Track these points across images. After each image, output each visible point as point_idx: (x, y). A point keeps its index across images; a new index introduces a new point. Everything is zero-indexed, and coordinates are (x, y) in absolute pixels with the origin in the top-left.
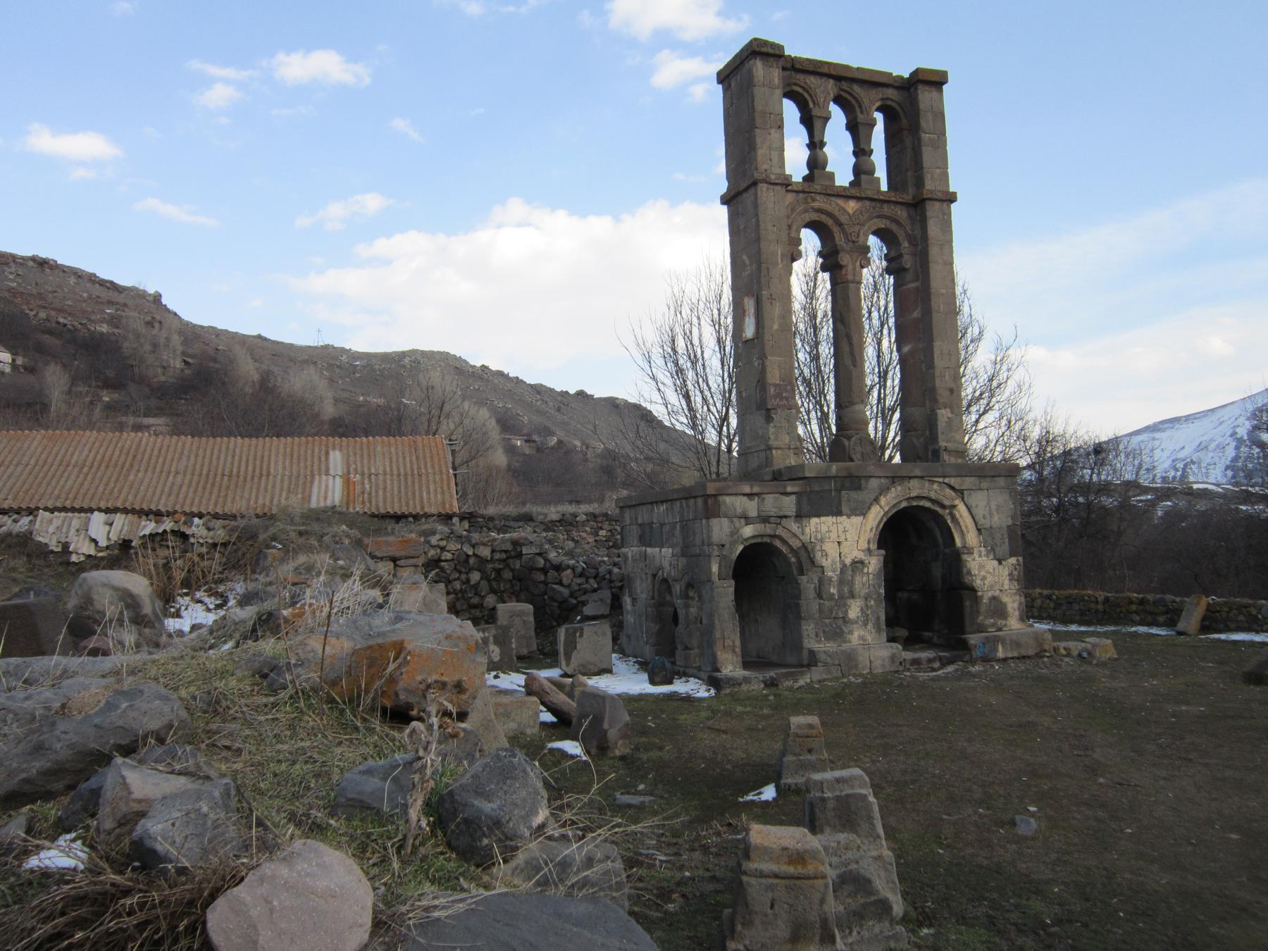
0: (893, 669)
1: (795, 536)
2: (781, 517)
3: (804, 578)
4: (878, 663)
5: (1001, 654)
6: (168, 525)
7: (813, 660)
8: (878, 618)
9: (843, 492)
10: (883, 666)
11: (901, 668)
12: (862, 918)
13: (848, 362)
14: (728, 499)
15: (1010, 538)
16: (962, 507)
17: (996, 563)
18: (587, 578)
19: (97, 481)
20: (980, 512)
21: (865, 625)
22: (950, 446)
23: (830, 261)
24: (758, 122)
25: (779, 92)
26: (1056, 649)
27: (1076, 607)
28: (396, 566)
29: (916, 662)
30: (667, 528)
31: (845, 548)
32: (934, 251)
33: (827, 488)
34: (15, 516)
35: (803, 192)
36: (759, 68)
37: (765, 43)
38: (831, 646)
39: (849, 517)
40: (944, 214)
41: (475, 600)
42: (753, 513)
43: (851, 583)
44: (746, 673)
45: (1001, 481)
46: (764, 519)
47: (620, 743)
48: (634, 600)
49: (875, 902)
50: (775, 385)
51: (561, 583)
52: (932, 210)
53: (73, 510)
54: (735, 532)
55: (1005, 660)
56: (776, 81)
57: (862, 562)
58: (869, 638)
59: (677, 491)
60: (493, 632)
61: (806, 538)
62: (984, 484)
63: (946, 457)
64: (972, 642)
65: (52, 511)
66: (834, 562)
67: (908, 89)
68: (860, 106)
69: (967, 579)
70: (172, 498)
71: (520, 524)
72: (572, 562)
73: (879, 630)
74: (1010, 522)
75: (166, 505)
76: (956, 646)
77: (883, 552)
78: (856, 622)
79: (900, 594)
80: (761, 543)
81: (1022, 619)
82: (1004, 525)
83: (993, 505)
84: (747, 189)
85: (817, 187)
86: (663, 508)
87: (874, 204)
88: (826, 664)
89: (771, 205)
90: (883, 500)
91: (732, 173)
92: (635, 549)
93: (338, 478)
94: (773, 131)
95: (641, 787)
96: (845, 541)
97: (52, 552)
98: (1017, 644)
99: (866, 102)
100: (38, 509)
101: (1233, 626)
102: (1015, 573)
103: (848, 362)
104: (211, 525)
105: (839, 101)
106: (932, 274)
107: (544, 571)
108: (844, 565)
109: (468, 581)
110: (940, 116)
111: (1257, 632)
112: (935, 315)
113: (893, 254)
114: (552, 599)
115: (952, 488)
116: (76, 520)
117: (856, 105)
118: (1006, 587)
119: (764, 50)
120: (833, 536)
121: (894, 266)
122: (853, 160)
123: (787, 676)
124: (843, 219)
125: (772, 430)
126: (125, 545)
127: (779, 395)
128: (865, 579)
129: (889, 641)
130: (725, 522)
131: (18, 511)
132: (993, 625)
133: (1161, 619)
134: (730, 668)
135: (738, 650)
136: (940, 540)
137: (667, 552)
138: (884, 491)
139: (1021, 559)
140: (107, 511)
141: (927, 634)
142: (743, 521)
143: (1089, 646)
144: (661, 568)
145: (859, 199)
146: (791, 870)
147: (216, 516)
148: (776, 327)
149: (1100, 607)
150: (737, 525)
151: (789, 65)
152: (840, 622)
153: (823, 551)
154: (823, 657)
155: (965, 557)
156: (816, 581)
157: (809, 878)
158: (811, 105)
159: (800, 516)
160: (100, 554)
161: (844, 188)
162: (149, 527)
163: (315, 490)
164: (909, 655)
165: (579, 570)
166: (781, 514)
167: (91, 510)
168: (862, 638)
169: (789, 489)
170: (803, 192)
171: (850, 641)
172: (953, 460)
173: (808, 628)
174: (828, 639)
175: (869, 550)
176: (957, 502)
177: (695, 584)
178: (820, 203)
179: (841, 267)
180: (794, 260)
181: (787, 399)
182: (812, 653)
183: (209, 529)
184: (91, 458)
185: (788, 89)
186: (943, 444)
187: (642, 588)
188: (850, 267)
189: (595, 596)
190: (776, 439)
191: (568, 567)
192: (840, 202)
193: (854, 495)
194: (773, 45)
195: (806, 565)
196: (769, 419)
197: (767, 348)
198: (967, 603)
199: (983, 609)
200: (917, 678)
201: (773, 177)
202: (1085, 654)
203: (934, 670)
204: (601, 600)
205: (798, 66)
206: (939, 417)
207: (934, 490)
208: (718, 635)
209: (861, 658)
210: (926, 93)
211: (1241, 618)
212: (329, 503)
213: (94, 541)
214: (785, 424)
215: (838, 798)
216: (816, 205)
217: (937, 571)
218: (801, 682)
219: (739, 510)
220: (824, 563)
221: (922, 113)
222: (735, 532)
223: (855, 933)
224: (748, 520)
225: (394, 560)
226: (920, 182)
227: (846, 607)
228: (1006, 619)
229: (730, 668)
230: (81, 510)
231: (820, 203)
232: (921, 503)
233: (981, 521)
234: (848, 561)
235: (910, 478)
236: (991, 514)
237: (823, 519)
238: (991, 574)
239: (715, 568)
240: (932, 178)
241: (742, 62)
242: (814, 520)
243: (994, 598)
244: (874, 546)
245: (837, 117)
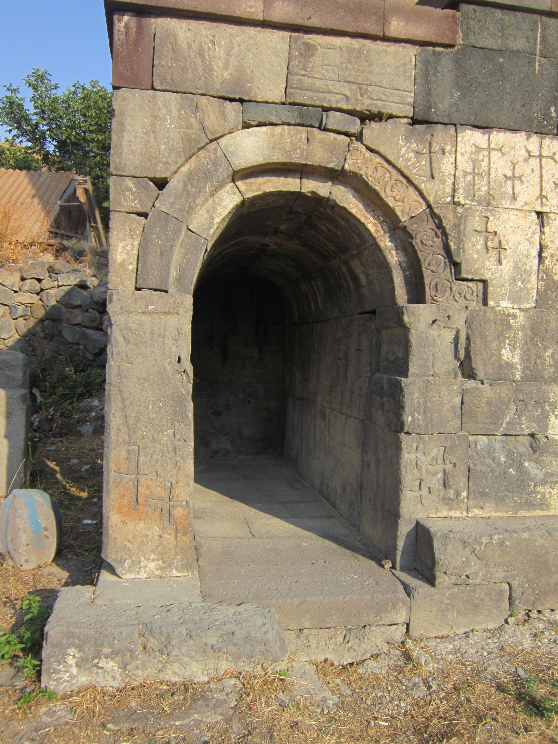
2: (366, 117)
33: (519, 44)
42: (270, 89)
66: (519, 271)
80: (299, 195)
120: (527, 193)
134: (152, 566)
153: (488, 234)
156: (460, 322)
166: (364, 104)
169: (396, 27)
171: (544, 505)
174: (479, 495)
220: (489, 269)
237: (499, 137)
242: (472, 138)
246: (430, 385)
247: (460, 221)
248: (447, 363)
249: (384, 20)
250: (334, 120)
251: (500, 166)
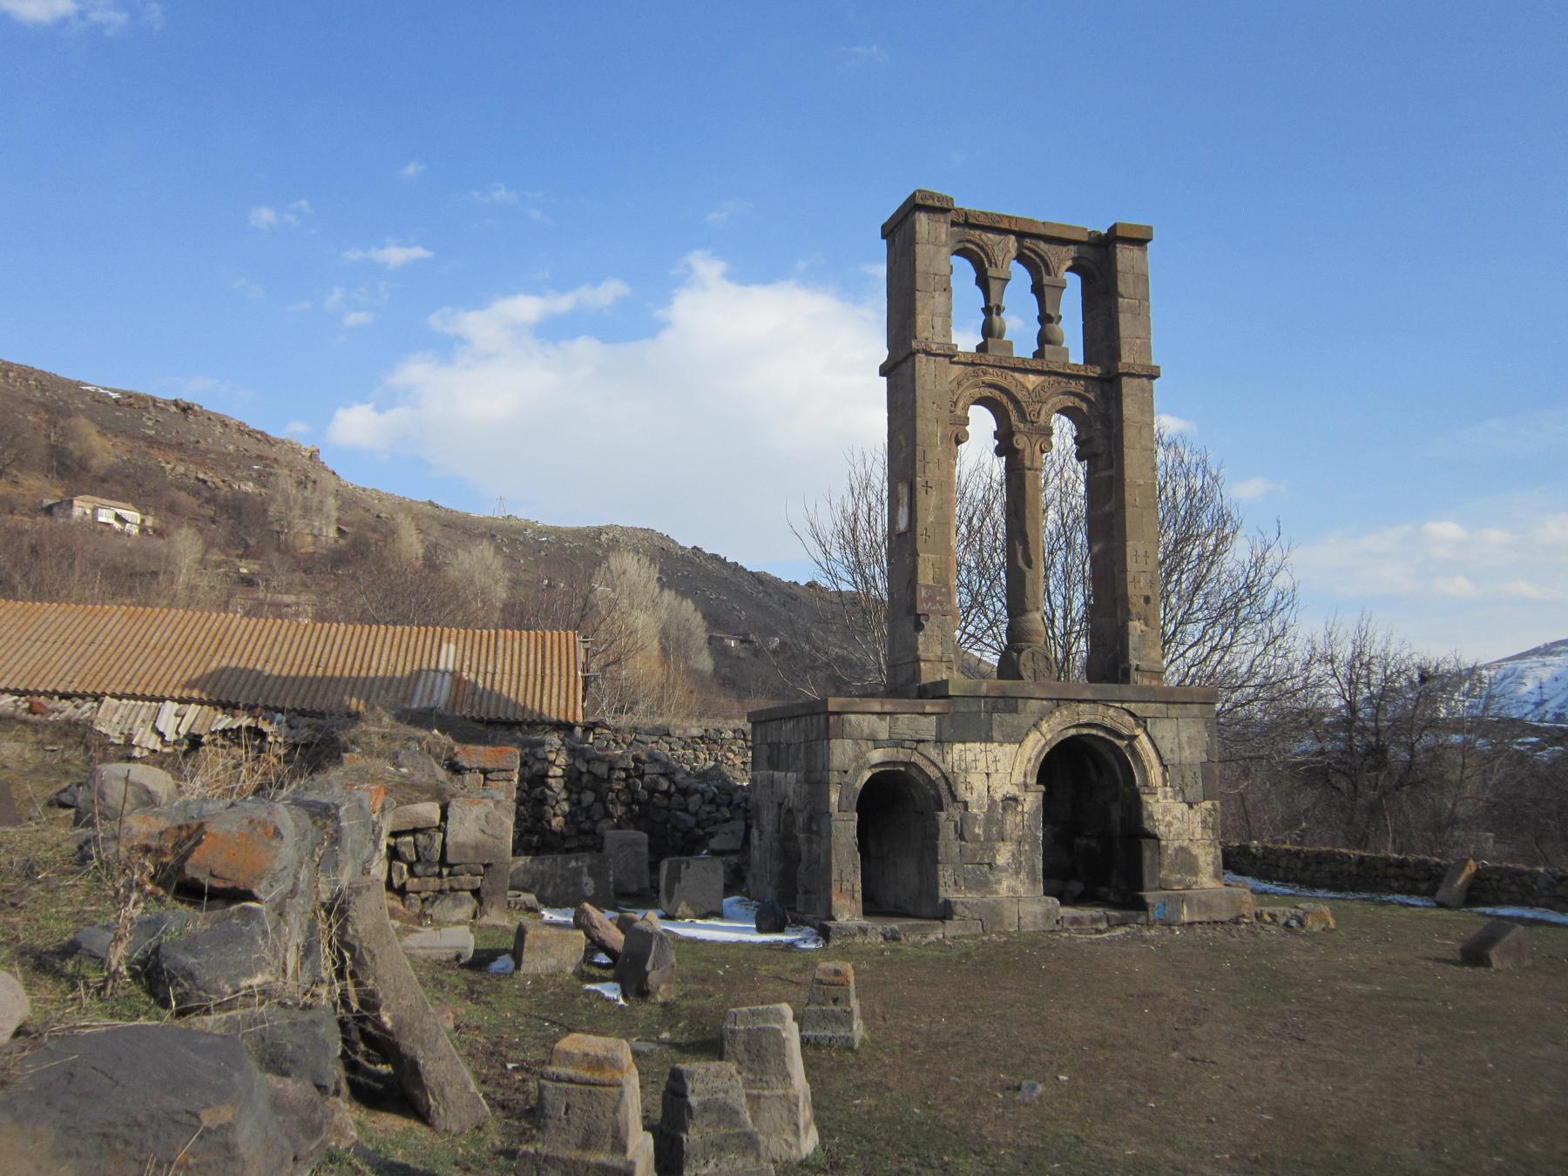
0: (1048, 928)
1: (934, 764)
2: (918, 741)
3: (943, 815)
4: (1027, 920)
5: (1186, 916)
6: (245, 721)
7: (945, 912)
8: (1033, 866)
9: (995, 715)
10: (1035, 924)
11: (1058, 928)
12: (722, 1149)
13: (1021, 563)
14: (852, 717)
15: (1204, 778)
16: (1143, 738)
17: (1185, 806)
18: (719, 806)
19: (175, 666)
20: (1165, 746)
21: (1017, 873)
22: (1143, 665)
23: (1005, 445)
24: (920, 282)
25: (945, 250)
26: (1259, 916)
27: (1326, 868)
28: (486, 779)
29: (1075, 921)
30: (792, 749)
31: (995, 780)
32: (1129, 434)
33: (975, 709)
34: (79, 701)
35: (973, 364)
36: (922, 221)
37: (932, 195)
38: (972, 896)
39: (1001, 744)
40: (1144, 391)
41: (587, 826)
42: (884, 736)
43: (1001, 823)
44: (864, 922)
45: (1195, 709)
46: (898, 743)
47: (662, 988)
48: (761, 833)
49: (738, 1135)
50: (927, 587)
51: (686, 810)
52: (1128, 386)
53: (143, 698)
54: (859, 756)
55: (1191, 924)
56: (943, 237)
57: (1015, 799)
58: (1021, 890)
59: (803, 705)
60: (588, 860)
61: (945, 768)
62: (1174, 711)
63: (1134, 675)
64: (1149, 900)
65: (120, 698)
66: (980, 796)
67: (1107, 247)
68: (1047, 266)
69: (1147, 825)
70: (256, 690)
71: (655, 738)
72: (702, 786)
73: (1034, 881)
74: (1204, 758)
75: (248, 697)
76: (1131, 902)
77: (1042, 787)
78: (1006, 870)
79: (1078, 841)
81: (1216, 876)
82: (1197, 762)
83: (1184, 737)
84: (905, 359)
85: (990, 358)
86: (791, 724)
88: (963, 918)
90: (1044, 726)
91: (891, 345)
92: (764, 772)
93: (447, 677)
95: (665, 1035)
96: (996, 773)
97: (112, 744)
98: (1206, 906)
99: (1053, 261)
100: (104, 694)
101: (1504, 897)
102: (1210, 820)
103: (1021, 563)
104: (294, 722)
105: (1020, 258)
106: (1127, 461)
107: (667, 794)
108: (993, 802)
109: (579, 802)
110: (1143, 278)
111: (1531, 906)
112: (1129, 511)
113: (1084, 437)
114: (674, 828)
115: (1132, 715)
116: (146, 708)
118: (1198, 836)
119: (929, 202)
120: (981, 765)
121: (1085, 450)
122: (1039, 327)
123: (913, 929)
125: (921, 639)
126: (195, 742)
127: (931, 599)
128: (1019, 818)
129: (1046, 893)
130: (849, 742)
131: (83, 696)
132: (1179, 882)
133: (1423, 887)
135: (859, 896)
136: (1120, 776)
137: (792, 776)
138: (1045, 715)
139: (1217, 803)
140: (181, 701)
141: (1104, 890)
142: (870, 744)
143: (1300, 913)
144: (786, 796)
146: (587, 1075)
147: (302, 713)
148: (931, 519)
149: (1354, 870)
150: (864, 748)
151: (961, 220)
152: (986, 868)
154: (959, 909)
155: (1144, 798)
157: (604, 1085)
159: (940, 741)
160: (167, 750)
161: (1024, 360)
162: (223, 721)
163: (420, 687)
164: (1068, 912)
165: (710, 795)
167: (163, 699)
168: (1011, 889)
169: (928, 709)
170: (973, 364)
172: (1146, 682)
173: (945, 875)
174: (969, 888)
175: (1026, 786)
176: (1138, 731)
177: (818, 815)
178: (992, 376)
179: (1017, 451)
180: (958, 442)
181: (941, 603)
182: (947, 903)
183: (291, 727)
184: (172, 641)
185: (960, 246)
186: (1134, 662)
187: (768, 818)
188: (1028, 451)
189: (726, 827)
190: (927, 650)
191: (696, 791)
192: (1018, 376)
193: (1008, 717)
194: (940, 198)
195: (946, 799)
196: (919, 627)
197: (920, 545)
198: (1147, 854)
199: (1166, 861)
200: (1074, 939)
201: (934, 347)
202: (1294, 923)
203: (1099, 931)
204: (733, 833)
205: (972, 220)
206: (1131, 630)
207: (1111, 716)
208: (835, 876)
209: (1007, 913)
211: (1513, 888)
212: (432, 705)
213: (162, 735)
214: (937, 632)
215: (749, 1031)
216: (988, 379)
217: (1116, 813)
218: (932, 938)
219: (866, 731)
220: (968, 797)
221: (1120, 275)
222: (859, 756)
223: (712, 1163)
224: (877, 743)
225: (485, 772)
226: (1115, 355)
227: (993, 851)
228: (1196, 875)
229: (847, 916)
230: (152, 699)
232: (1094, 732)
233: (1167, 756)
234: (998, 797)
235: (1080, 701)
236: (1180, 748)
237: (969, 745)
238: (1178, 820)
239: (834, 798)
241: (906, 216)
242: (958, 747)
243: (1181, 849)
244: (1032, 780)
245: (1020, 277)
246: (948, 843)
247: (955, 779)
248: (952, 835)
249: (923, 706)
250: (907, 744)
251: (970, 756)
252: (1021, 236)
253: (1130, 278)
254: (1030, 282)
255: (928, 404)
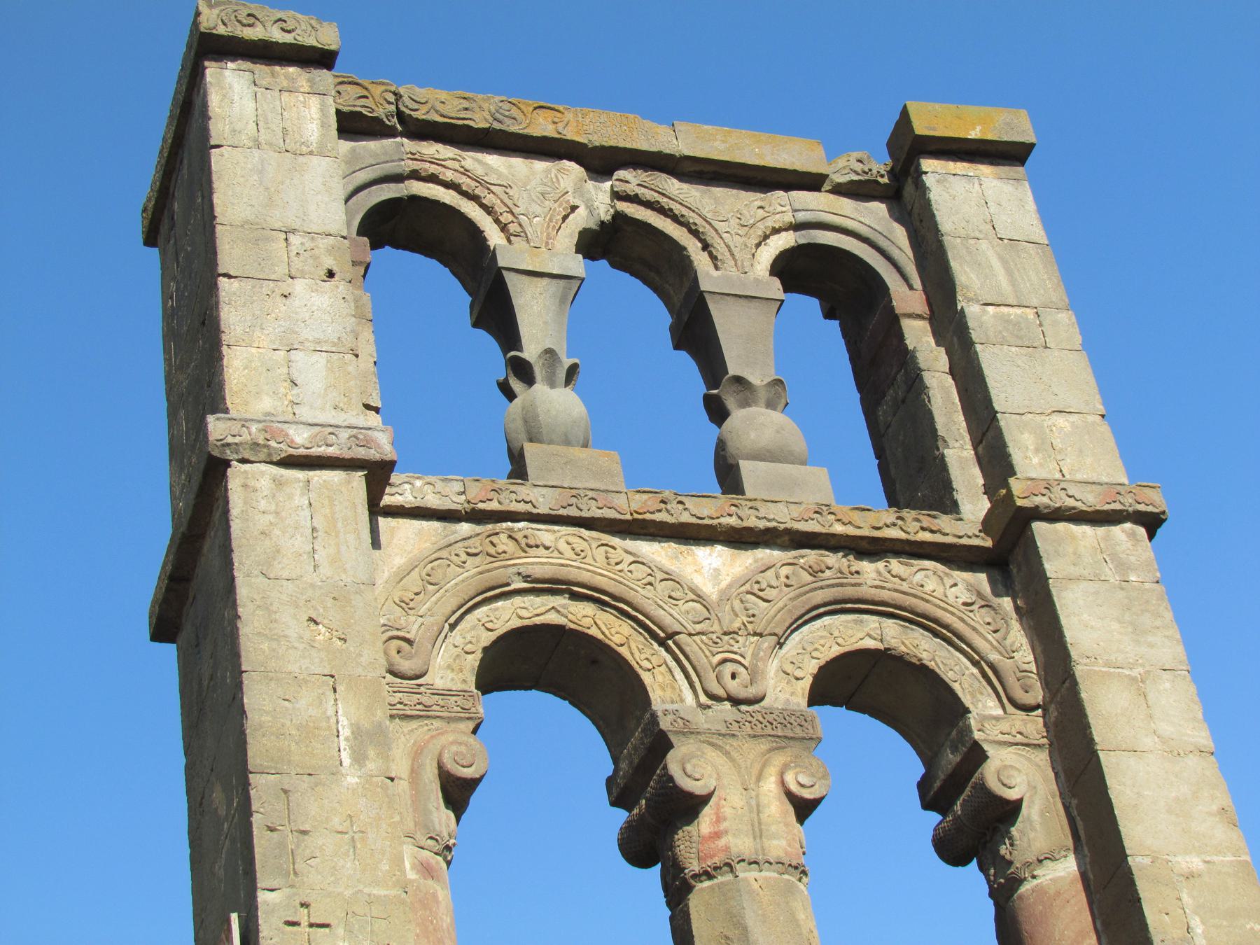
24: (230, 254)
36: (231, 90)
40: (1122, 567)
87: (810, 556)
89: (300, 543)
94: (299, 286)
117: (692, 246)
124: (674, 616)
145: (740, 539)
158: (495, 238)
170: (477, 516)
178: (561, 550)
210: (959, 186)
216: (539, 564)
231: (561, 550)
240: (1045, 446)
252: (601, 162)
253: (988, 251)
254: (666, 319)
255: (292, 625)
